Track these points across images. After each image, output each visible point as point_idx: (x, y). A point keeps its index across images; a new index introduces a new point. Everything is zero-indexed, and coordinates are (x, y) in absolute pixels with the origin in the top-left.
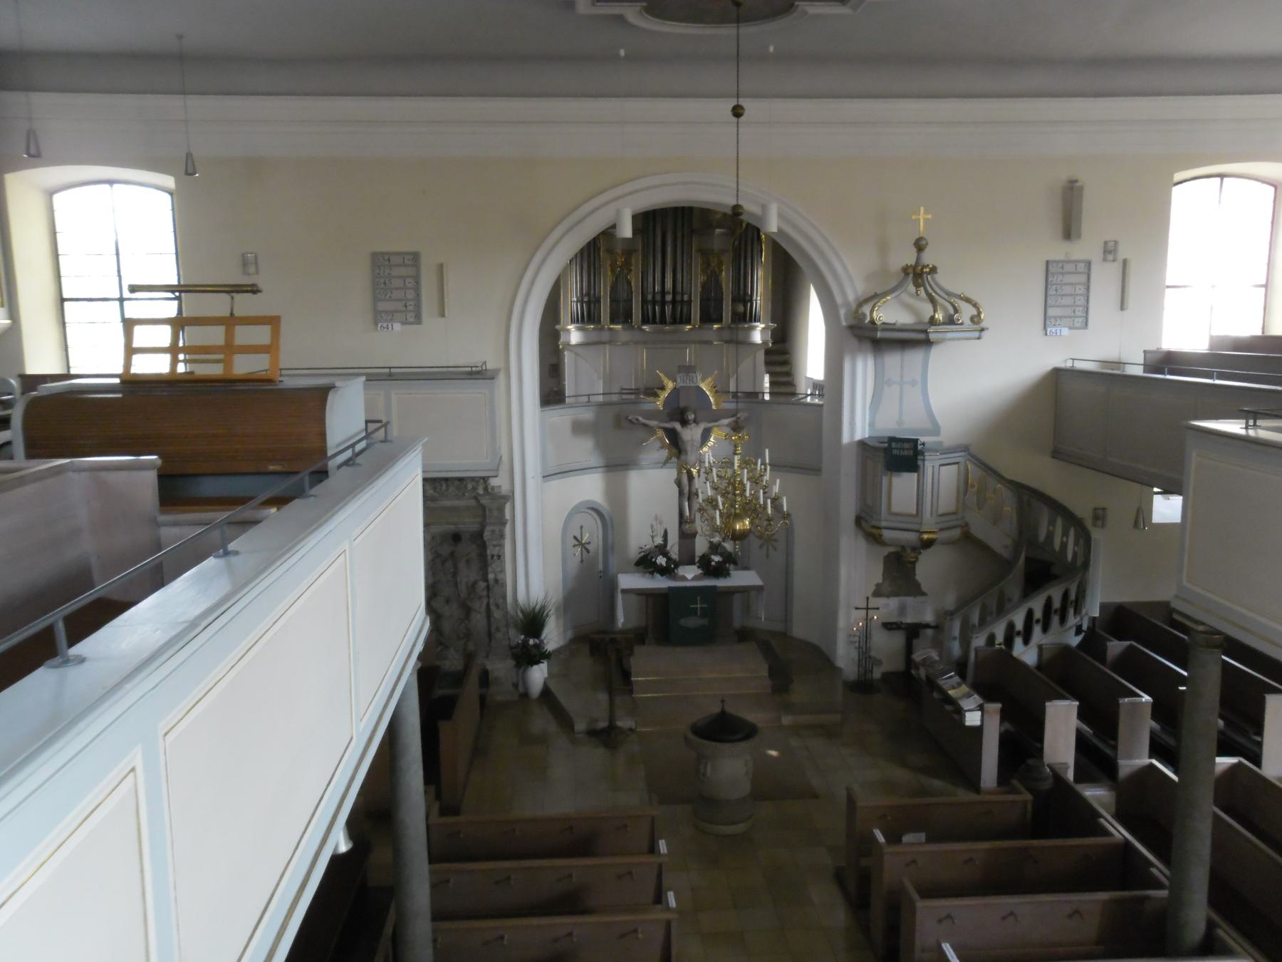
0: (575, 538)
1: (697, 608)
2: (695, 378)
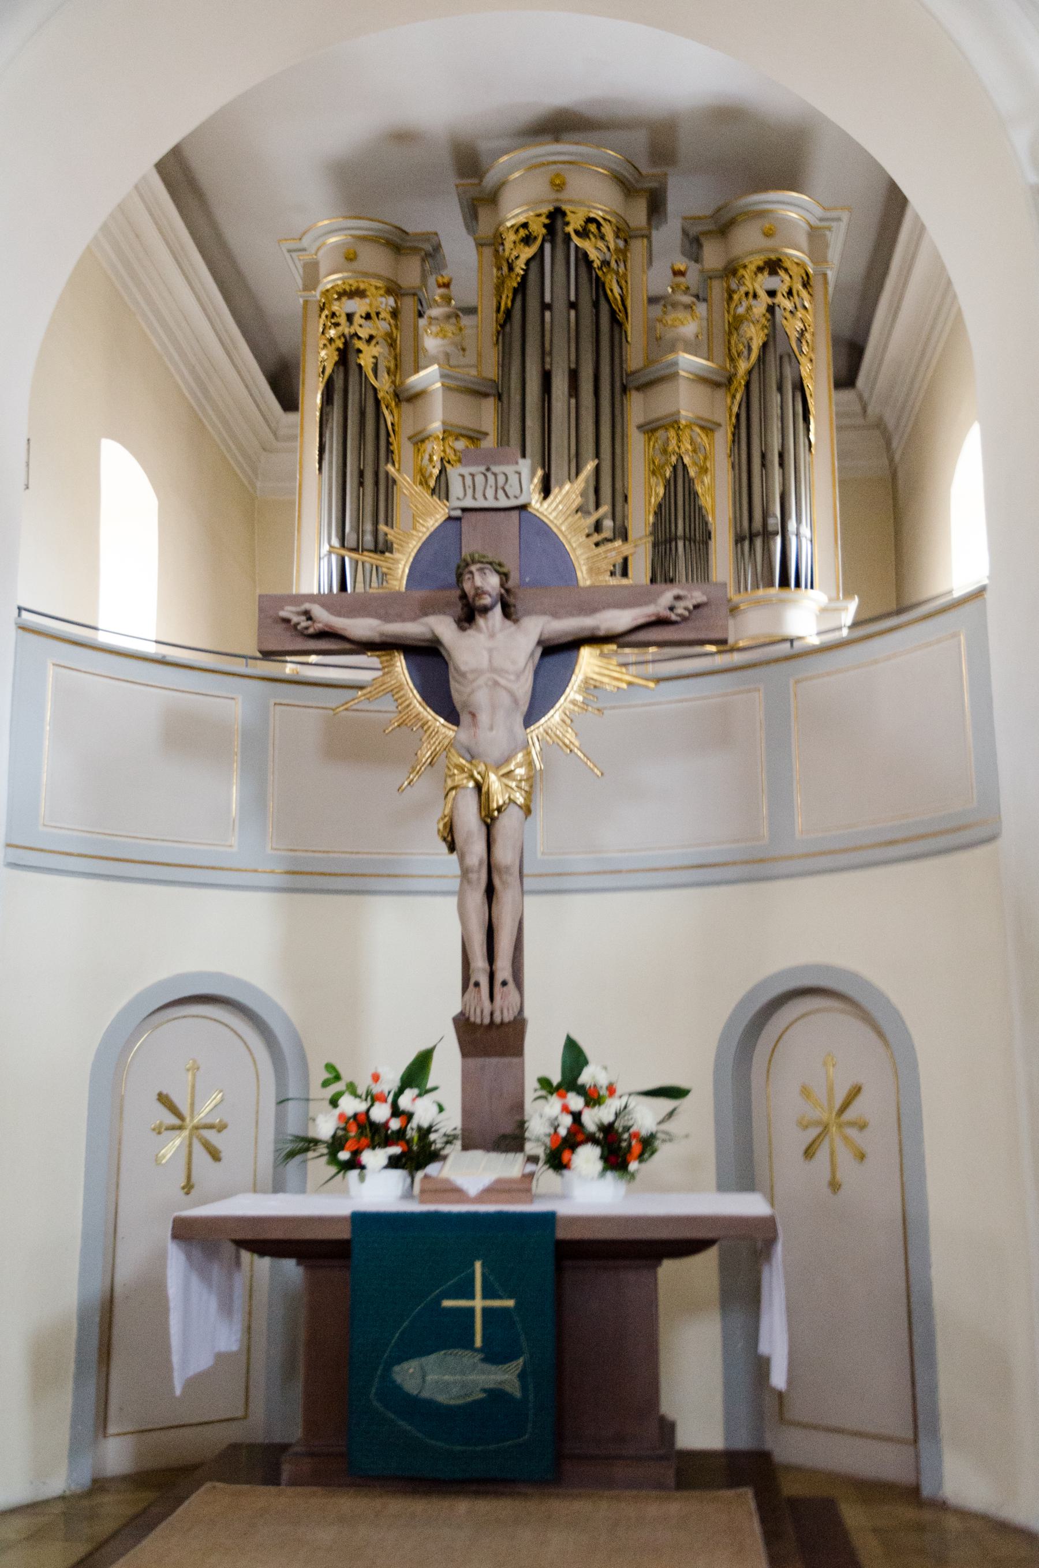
0: (164, 1100)
1: (471, 1311)
2: (513, 479)
